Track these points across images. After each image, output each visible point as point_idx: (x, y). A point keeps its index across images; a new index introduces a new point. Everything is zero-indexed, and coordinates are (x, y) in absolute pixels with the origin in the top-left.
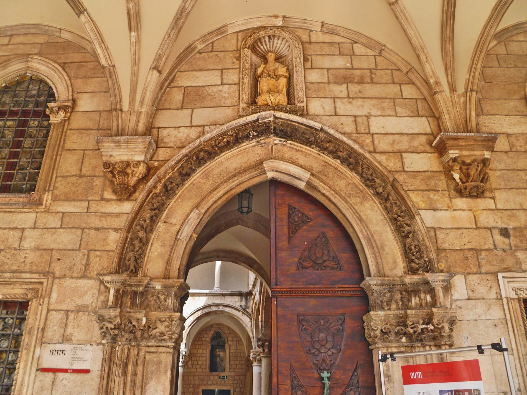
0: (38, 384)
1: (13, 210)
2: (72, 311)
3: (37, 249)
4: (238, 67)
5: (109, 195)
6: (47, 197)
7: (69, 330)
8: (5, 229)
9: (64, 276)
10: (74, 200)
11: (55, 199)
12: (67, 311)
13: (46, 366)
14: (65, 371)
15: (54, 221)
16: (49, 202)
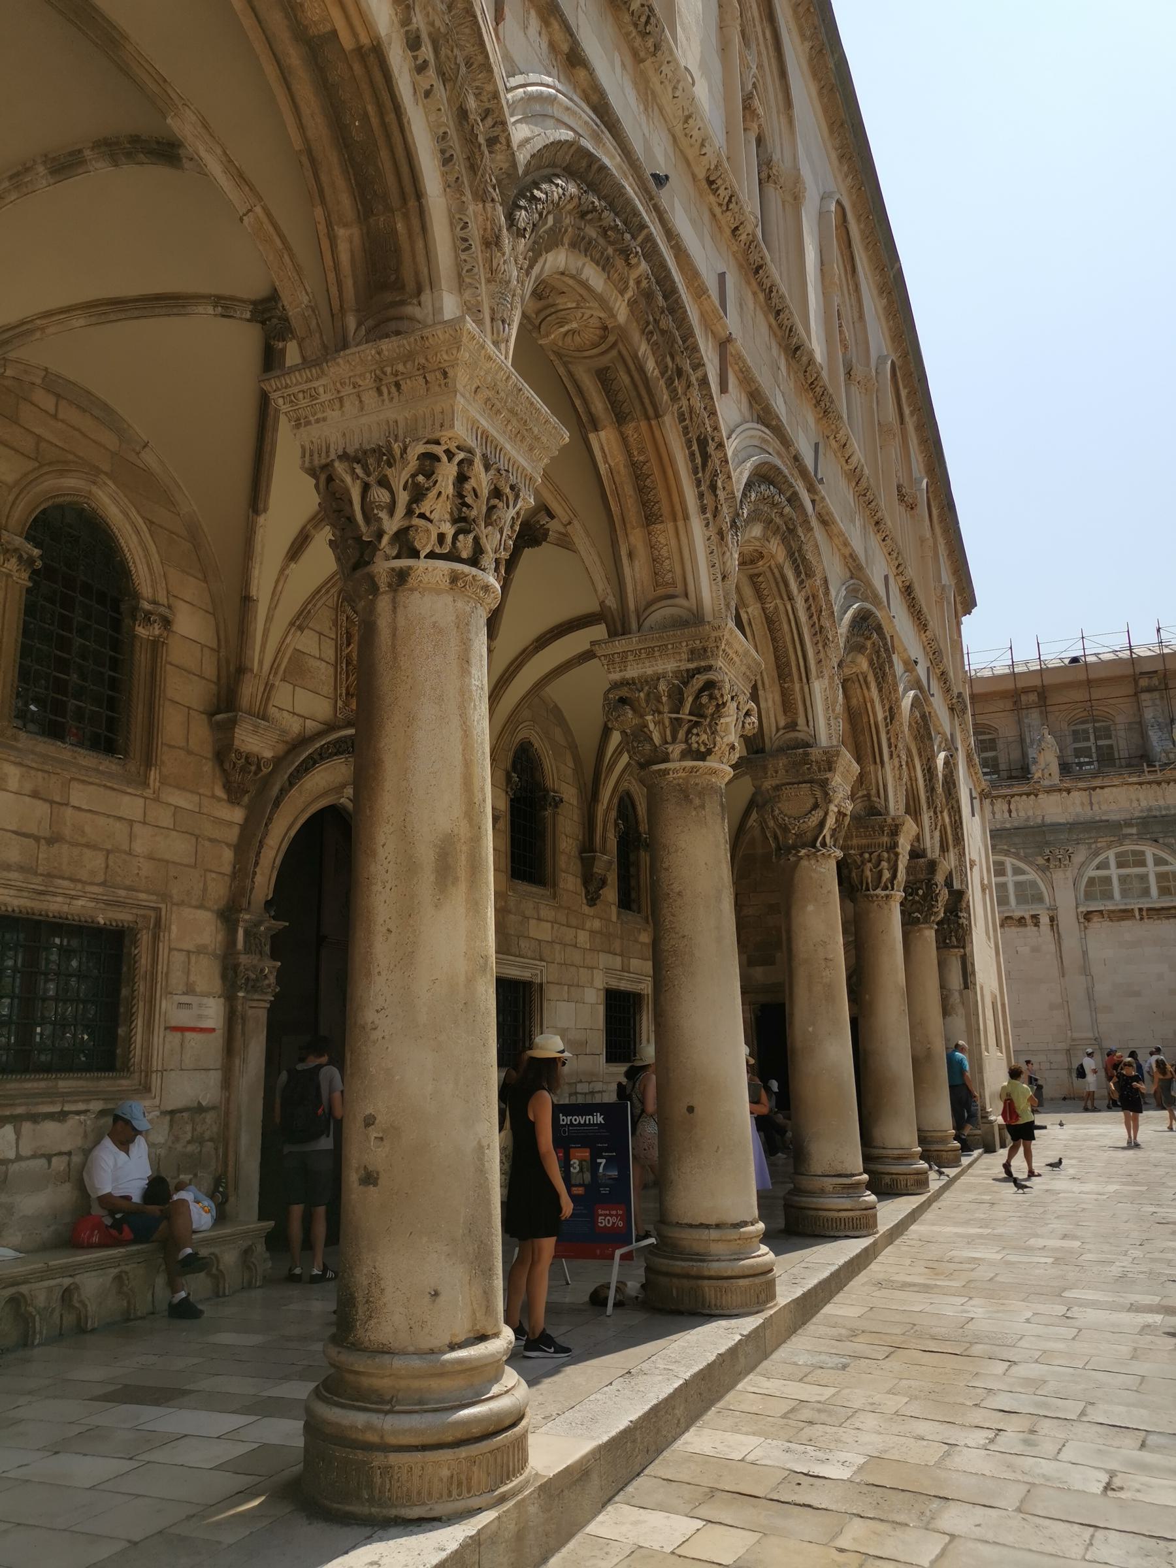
0: (167, 1046)
1: (115, 786)
2: (194, 952)
3: (150, 858)
4: (334, 637)
5: (220, 793)
6: (153, 774)
7: (192, 978)
8: (109, 816)
9: (182, 903)
10: (184, 789)
11: (164, 782)
12: (189, 952)
13: (173, 1024)
14: (193, 1029)
15: (166, 820)
16: (157, 784)
